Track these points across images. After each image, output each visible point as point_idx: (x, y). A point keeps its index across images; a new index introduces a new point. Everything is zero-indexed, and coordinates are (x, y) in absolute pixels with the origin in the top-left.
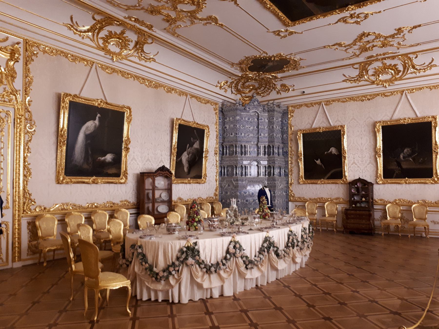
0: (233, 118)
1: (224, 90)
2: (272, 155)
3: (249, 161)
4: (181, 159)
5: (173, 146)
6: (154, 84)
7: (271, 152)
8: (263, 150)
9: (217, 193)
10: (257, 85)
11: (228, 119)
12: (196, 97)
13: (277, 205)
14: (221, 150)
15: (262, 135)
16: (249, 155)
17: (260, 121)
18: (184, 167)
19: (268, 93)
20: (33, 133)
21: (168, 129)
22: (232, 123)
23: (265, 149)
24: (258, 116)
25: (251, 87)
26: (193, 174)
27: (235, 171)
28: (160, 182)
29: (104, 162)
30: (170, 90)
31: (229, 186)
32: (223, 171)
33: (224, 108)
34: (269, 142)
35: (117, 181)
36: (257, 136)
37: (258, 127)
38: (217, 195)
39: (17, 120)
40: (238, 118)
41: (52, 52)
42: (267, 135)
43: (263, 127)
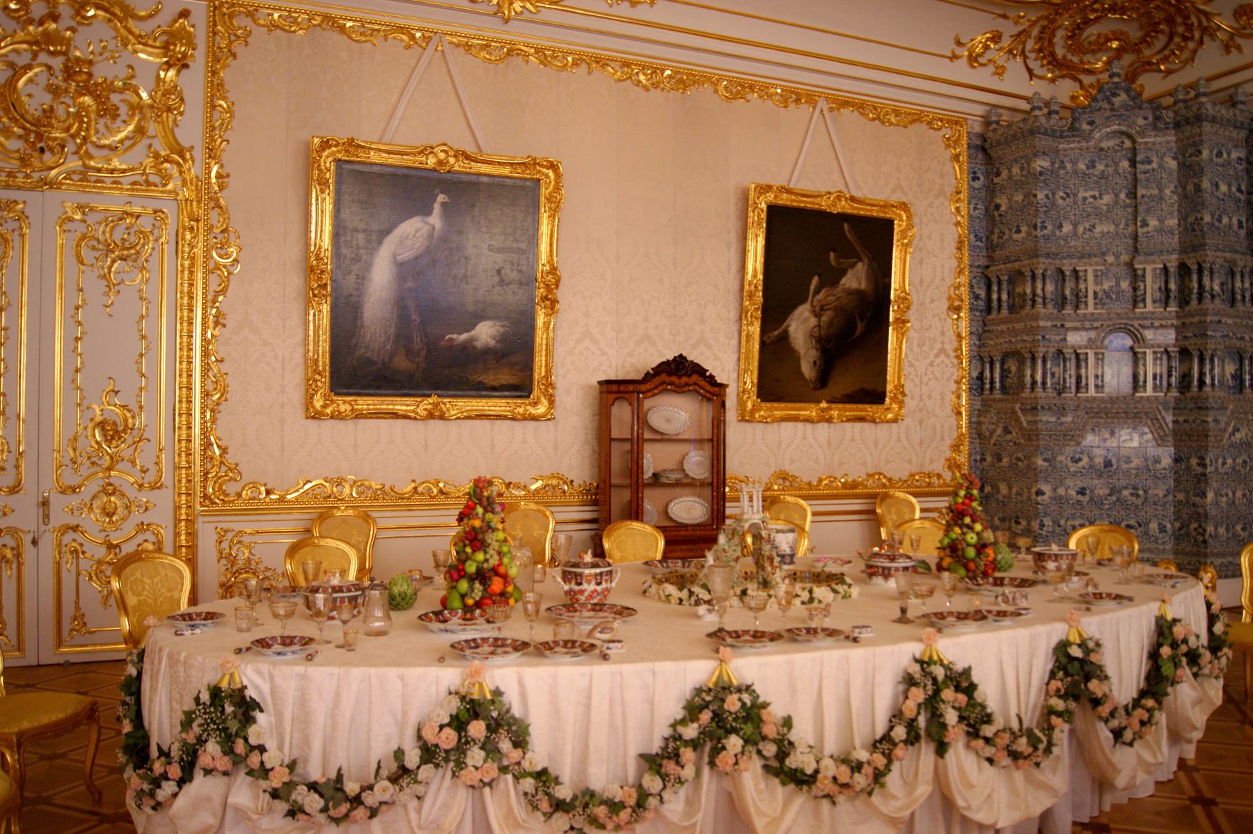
0: (1022, 169)
1: (991, 68)
2: (1194, 302)
3: (1093, 334)
4: (786, 332)
5: (747, 287)
6: (670, 77)
7: (1190, 290)
8: (1160, 283)
9: (963, 458)
10: (1135, 33)
11: (1005, 174)
12: (860, 107)
13: (1213, 512)
14: (983, 293)
15: (1153, 223)
16: (1091, 308)
17: (1140, 167)
18: (799, 359)
19: (1185, 55)
20: (231, 269)
21: (733, 225)
22: (1019, 185)
23: (1166, 282)
24: (1134, 151)
25: (1115, 45)
26: (844, 381)
27: (1029, 372)
28: (675, 413)
29: (467, 348)
30: (741, 89)
31: (1007, 431)
32: (987, 374)
33: (990, 134)
34: (1183, 251)
35: (521, 410)
36: (1131, 229)
37: (1133, 194)
38: (959, 467)
39: (183, 234)
40: (1041, 163)
41: (295, 21)
42: (1173, 222)
43: (1155, 192)
